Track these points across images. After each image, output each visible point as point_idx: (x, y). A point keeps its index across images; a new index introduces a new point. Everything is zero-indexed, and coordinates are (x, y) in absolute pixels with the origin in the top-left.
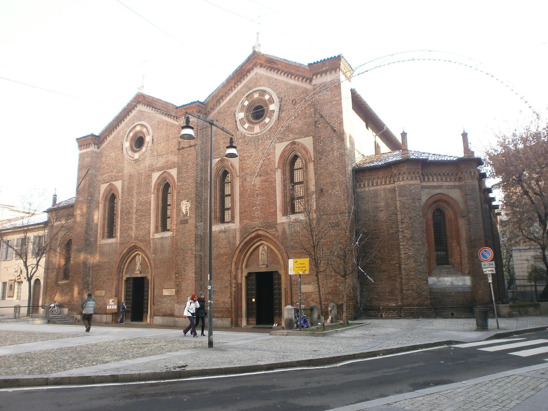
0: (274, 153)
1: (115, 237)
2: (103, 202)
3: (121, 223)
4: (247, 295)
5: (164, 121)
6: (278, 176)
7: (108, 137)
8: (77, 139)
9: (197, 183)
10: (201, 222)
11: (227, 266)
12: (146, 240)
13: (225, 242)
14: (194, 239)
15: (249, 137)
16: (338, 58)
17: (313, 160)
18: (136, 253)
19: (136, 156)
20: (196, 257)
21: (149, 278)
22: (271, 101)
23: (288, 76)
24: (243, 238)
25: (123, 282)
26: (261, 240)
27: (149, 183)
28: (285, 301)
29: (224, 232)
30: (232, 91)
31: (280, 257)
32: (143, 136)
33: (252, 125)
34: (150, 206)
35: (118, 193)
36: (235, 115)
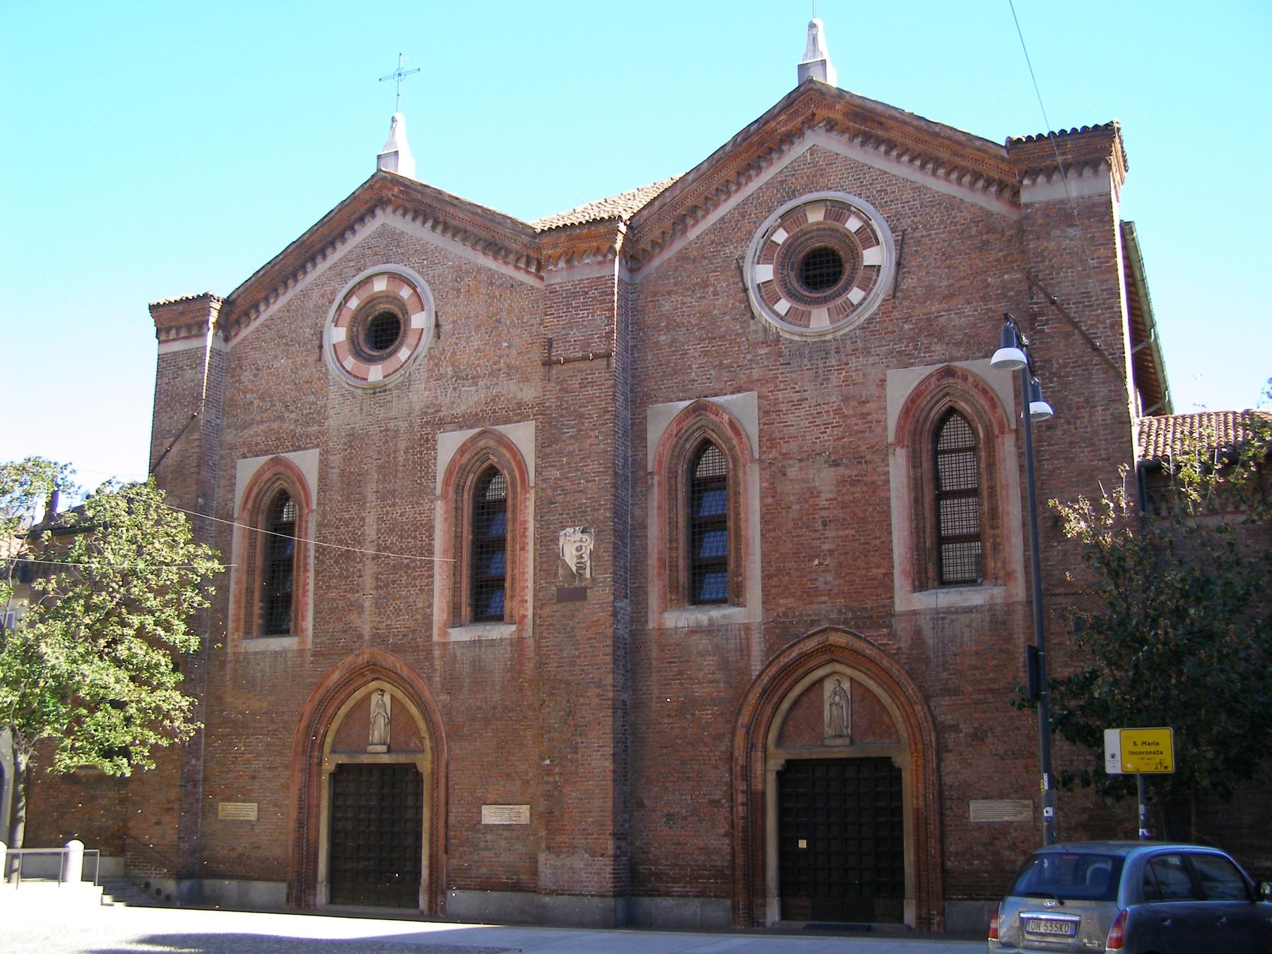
0: (882, 398)
1: (298, 631)
2: (246, 515)
3: (317, 587)
4: (782, 826)
5: (480, 270)
6: (898, 469)
7: (262, 308)
8: (153, 308)
9: (616, 473)
10: (625, 597)
11: (717, 738)
12: (416, 645)
13: (710, 662)
14: (609, 650)
15: (791, 342)
16: (1105, 134)
17: (1013, 426)
18: (374, 685)
19: (375, 373)
20: (615, 708)
21: (425, 764)
22: (868, 237)
23: (923, 166)
24: (773, 652)
25: (325, 778)
26: (833, 660)
27: (424, 466)
28: (918, 846)
29: (710, 630)
30: (729, 194)
31: (896, 713)
32: (396, 310)
33: (801, 307)
34: (431, 537)
35: (305, 488)
36: (740, 270)
